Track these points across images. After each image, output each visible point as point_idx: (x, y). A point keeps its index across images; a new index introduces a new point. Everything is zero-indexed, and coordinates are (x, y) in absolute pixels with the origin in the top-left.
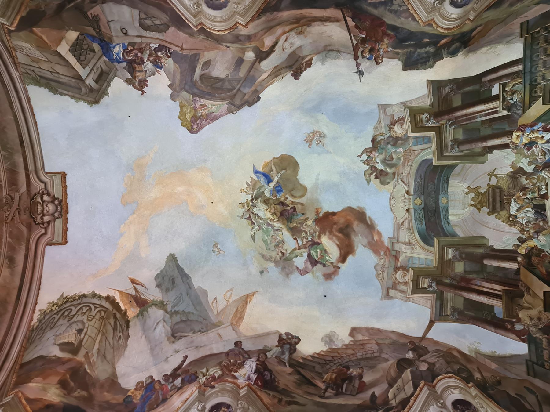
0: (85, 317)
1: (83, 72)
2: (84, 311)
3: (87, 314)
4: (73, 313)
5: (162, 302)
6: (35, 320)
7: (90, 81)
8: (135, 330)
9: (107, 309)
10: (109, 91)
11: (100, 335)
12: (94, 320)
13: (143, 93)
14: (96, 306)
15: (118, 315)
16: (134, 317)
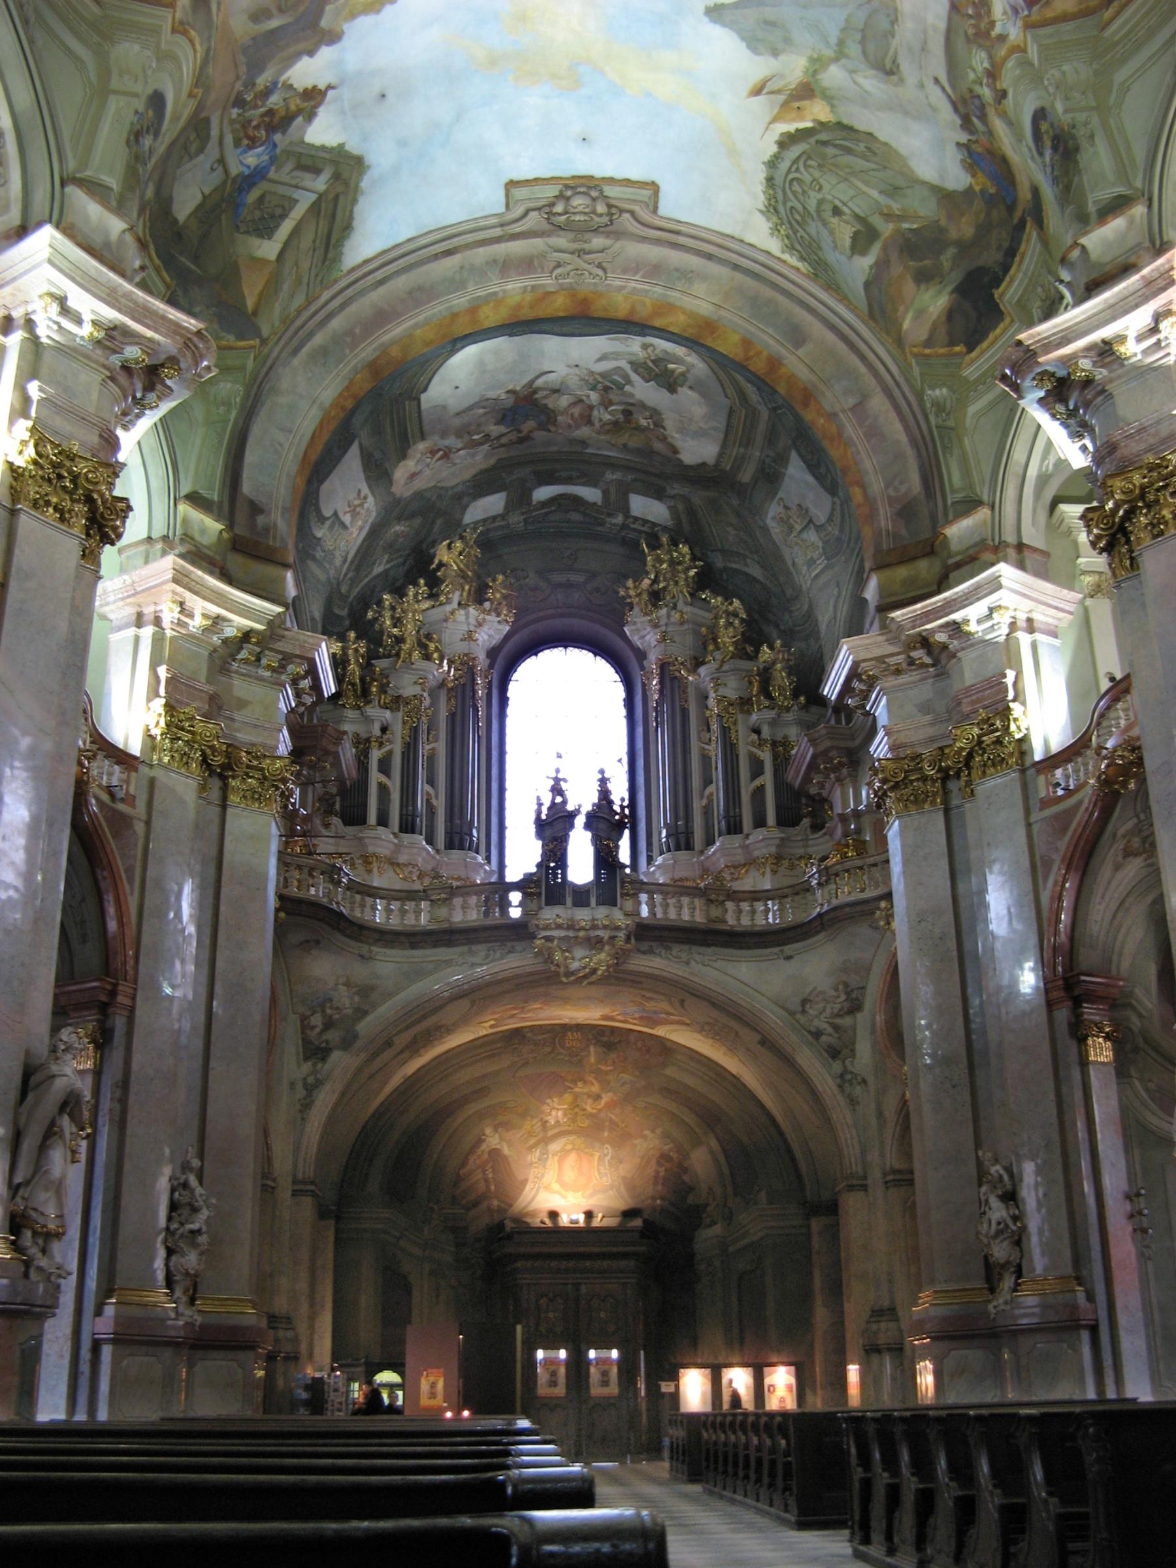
0: (812, 194)
1: (305, 201)
2: (800, 190)
3: (806, 189)
4: (800, 207)
5: (812, 60)
6: (800, 265)
7: (321, 183)
8: (862, 120)
9: (804, 153)
10: (334, 144)
11: (853, 179)
12: (821, 181)
13: (330, 87)
14: (793, 169)
15: (823, 137)
16: (832, 111)
